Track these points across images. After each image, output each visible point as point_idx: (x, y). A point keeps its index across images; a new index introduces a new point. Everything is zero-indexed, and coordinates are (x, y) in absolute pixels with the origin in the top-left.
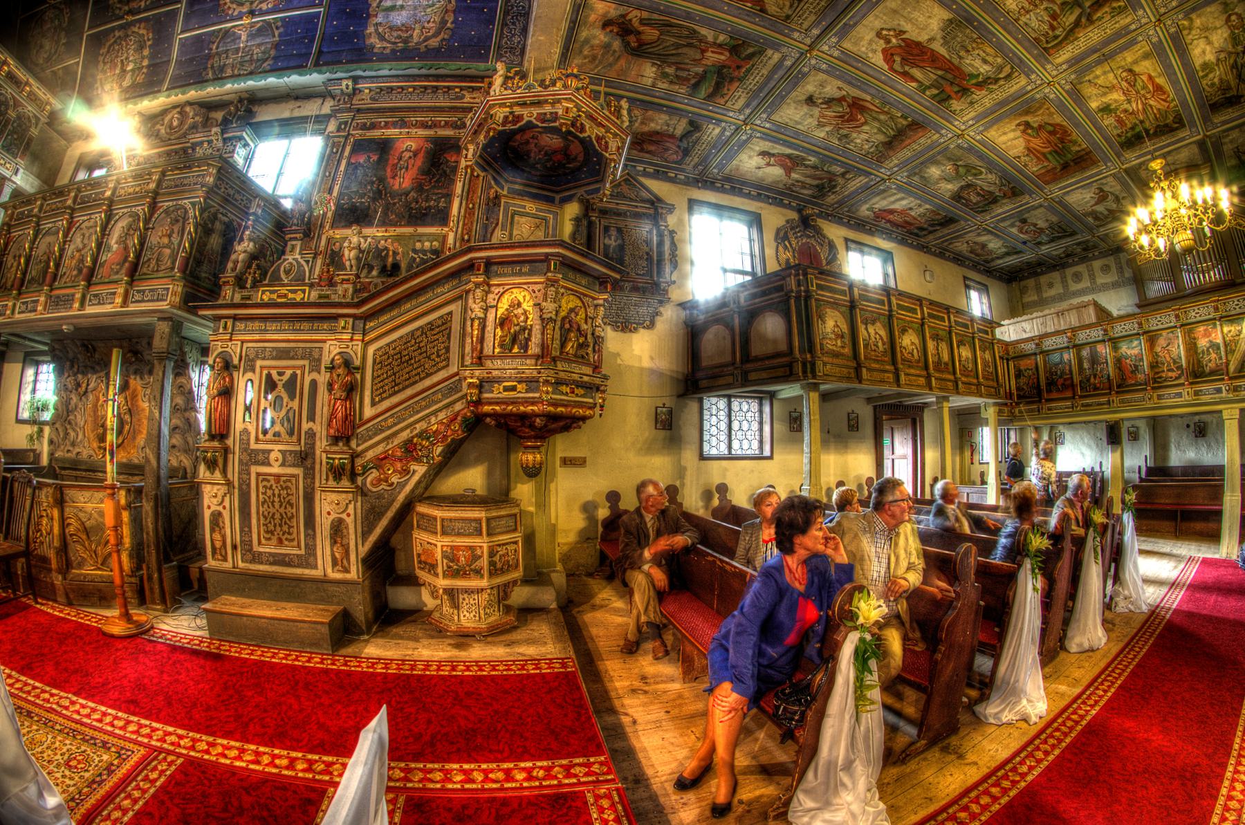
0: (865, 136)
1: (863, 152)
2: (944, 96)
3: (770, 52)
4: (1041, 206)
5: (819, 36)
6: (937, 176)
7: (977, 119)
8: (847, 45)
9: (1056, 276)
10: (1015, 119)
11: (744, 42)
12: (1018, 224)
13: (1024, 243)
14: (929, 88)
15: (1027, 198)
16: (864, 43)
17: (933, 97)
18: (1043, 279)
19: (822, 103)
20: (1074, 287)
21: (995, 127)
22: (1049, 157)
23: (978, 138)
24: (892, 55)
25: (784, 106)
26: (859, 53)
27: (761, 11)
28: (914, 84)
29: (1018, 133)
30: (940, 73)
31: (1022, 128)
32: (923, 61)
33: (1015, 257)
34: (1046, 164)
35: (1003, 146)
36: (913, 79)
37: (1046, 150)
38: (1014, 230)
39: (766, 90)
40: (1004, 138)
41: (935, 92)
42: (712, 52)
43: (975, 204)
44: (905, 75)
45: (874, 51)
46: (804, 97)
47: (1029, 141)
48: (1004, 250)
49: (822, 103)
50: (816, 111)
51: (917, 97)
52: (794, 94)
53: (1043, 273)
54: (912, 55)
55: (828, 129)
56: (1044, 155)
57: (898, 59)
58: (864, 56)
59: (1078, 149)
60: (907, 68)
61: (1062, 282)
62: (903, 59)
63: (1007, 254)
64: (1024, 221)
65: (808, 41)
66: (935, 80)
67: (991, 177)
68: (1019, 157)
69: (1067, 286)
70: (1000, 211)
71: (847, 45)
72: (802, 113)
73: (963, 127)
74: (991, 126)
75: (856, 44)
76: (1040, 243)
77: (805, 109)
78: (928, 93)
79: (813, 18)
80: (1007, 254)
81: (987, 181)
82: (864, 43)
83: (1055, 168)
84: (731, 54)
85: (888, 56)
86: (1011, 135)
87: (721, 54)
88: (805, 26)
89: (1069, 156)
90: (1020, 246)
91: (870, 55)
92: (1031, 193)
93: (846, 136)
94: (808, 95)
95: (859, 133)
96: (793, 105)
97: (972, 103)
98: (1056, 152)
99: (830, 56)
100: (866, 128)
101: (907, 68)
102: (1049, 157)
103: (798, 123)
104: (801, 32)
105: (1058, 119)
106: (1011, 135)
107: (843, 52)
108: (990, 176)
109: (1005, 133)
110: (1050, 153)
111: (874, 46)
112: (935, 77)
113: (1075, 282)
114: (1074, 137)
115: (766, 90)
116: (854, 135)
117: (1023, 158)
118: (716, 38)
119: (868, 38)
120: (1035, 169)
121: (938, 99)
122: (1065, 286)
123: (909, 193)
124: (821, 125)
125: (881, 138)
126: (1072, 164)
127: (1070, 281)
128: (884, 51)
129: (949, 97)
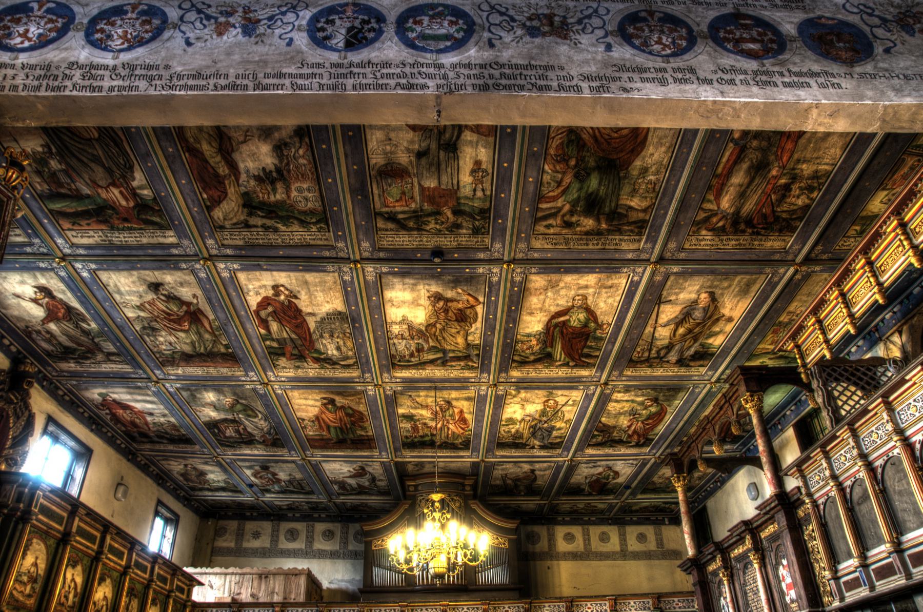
0: (172, 339)
1: (155, 350)
2: (280, 352)
3: (171, 233)
4: (293, 462)
5: (227, 256)
6: (209, 401)
7: (291, 380)
8: (242, 277)
9: (267, 526)
10: (324, 393)
11: (160, 210)
12: (257, 468)
13: (251, 486)
14: (273, 340)
15: (284, 451)
16: (257, 284)
17: (268, 348)
18: (250, 526)
19: (164, 295)
20: (285, 545)
21: (301, 391)
22: (332, 430)
23: (279, 392)
24: (269, 304)
25: (125, 273)
26: (244, 287)
27: (207, 207)
28: (263, 331)
29: (319, 404)
30: (293, 336)
31: (325, 401)
32: (289, 322)
33: (230, 494)
34: (324, 433)
35: (296, 407)
36: (267, 328)
37: (332, 424)
38: (248, 472)
39: (127, 252)
40: (303, 402)
41: (275, 345)
42: (121, 192)
43: (226, 437)
44: (264, 323)
45: (257, 293)
46: (153, 280)
47: (322, 412)
48: (222, 484)
49: (164, 295)
50: (150, 296)
51: (255, 341)
52: (147, 272)
53: (252, 518)
54: (284, 313)
55: (142, 314)
56: (328, 427)
57: (270, 309)
58: (245, 291)
59: (363, 433)
60: (270, 318)
61: (272, 536)
62: (274, 312)
63: (223, 489)
64: (265, 468)
65: (214, 252)
66: (285, 339)
67: (263, 424)
68: (303, 420)
69: (277, 541)
70: (248, 452)
71: (242, 277)
72: (134, 289)
73: (273, 379)
74: (298, 388)
75: (249, 280)
76: (268, 491)
77: (142, 289)
78: (268, 343)
79: (241, 243)
80: (223, 489)
81: (257, 425)
82: (257, 284)
83: (331, 440)
84: (134, 207)
85: (265, 303)
86: (311, 402)
87: (126, 199)
88: (225, 242)
89: (351, 436)
90: (244, 487)
91: (251, 293)
92: (291, 449)
93: (154, 329)
94: (160, 281)
95: (171, 334)
96: (135, 278)
97: (298, 367)
98: (341, 429)
99: (218, 273)
100: (182, 335)
101: (270, 318)
102: (332, 430)
103: (119, 292)
104: (217, 242)
105: (362, 408)
106: (311, 402)
107: (231, 277)
108: (262, 422)
109: (306, 399)
110: (335, 428)
111: (262, 291)
112: (285, 335)
113: (287, 540)
114: (366, 424)
115: (127, 252)
116: (163, 333)
117: (306, 422)
118: (141, 188)
119: (264, 282)
120: (311, 433)
121: (272, 350)
122: (275, 539)
123: (163, 401)
124: (141, 307)
125: (187, 349)
126: (349, 442)
127: (282, 537)
128: (266, 299)
129: (283, 355)
